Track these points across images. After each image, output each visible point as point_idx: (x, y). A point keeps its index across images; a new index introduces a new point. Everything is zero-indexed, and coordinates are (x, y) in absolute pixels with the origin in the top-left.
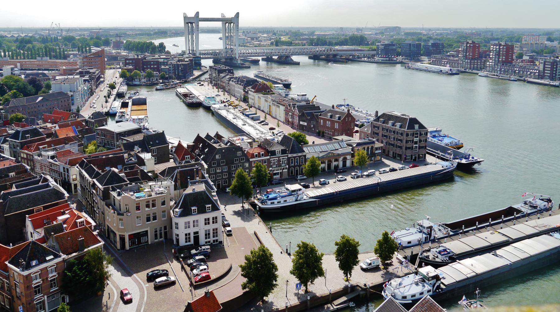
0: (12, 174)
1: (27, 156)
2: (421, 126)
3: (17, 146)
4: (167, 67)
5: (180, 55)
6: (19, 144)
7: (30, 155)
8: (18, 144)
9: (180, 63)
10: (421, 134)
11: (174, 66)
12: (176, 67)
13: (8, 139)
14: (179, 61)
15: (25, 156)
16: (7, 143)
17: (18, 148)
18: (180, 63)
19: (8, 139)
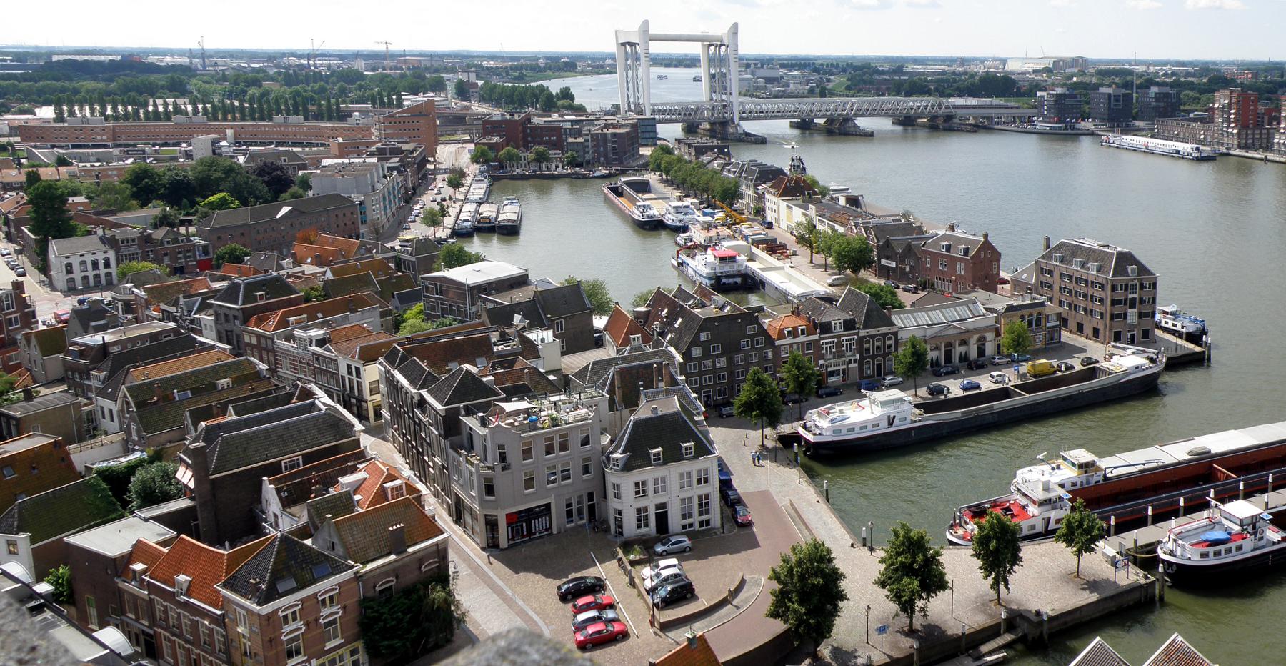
0: (224, 382)
1: (259, 341)
2: (1142, 270)
3: (235, 318)
4: (580, 140)
5: (607, 113)
6: (240, 314)
7: (266, 338)
8: (237, 313)
9: (611, 131)
10: (1142, 287)
11: (595, 138)
12: (600, 140)
13: (212, 301)
14: (607, 126)
15: (254, 341)
16: (211, 311)
17: (237, 322)
18: (611, 131)
19: (212, 301)
